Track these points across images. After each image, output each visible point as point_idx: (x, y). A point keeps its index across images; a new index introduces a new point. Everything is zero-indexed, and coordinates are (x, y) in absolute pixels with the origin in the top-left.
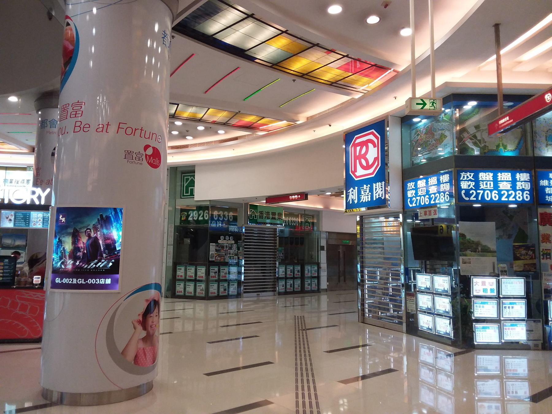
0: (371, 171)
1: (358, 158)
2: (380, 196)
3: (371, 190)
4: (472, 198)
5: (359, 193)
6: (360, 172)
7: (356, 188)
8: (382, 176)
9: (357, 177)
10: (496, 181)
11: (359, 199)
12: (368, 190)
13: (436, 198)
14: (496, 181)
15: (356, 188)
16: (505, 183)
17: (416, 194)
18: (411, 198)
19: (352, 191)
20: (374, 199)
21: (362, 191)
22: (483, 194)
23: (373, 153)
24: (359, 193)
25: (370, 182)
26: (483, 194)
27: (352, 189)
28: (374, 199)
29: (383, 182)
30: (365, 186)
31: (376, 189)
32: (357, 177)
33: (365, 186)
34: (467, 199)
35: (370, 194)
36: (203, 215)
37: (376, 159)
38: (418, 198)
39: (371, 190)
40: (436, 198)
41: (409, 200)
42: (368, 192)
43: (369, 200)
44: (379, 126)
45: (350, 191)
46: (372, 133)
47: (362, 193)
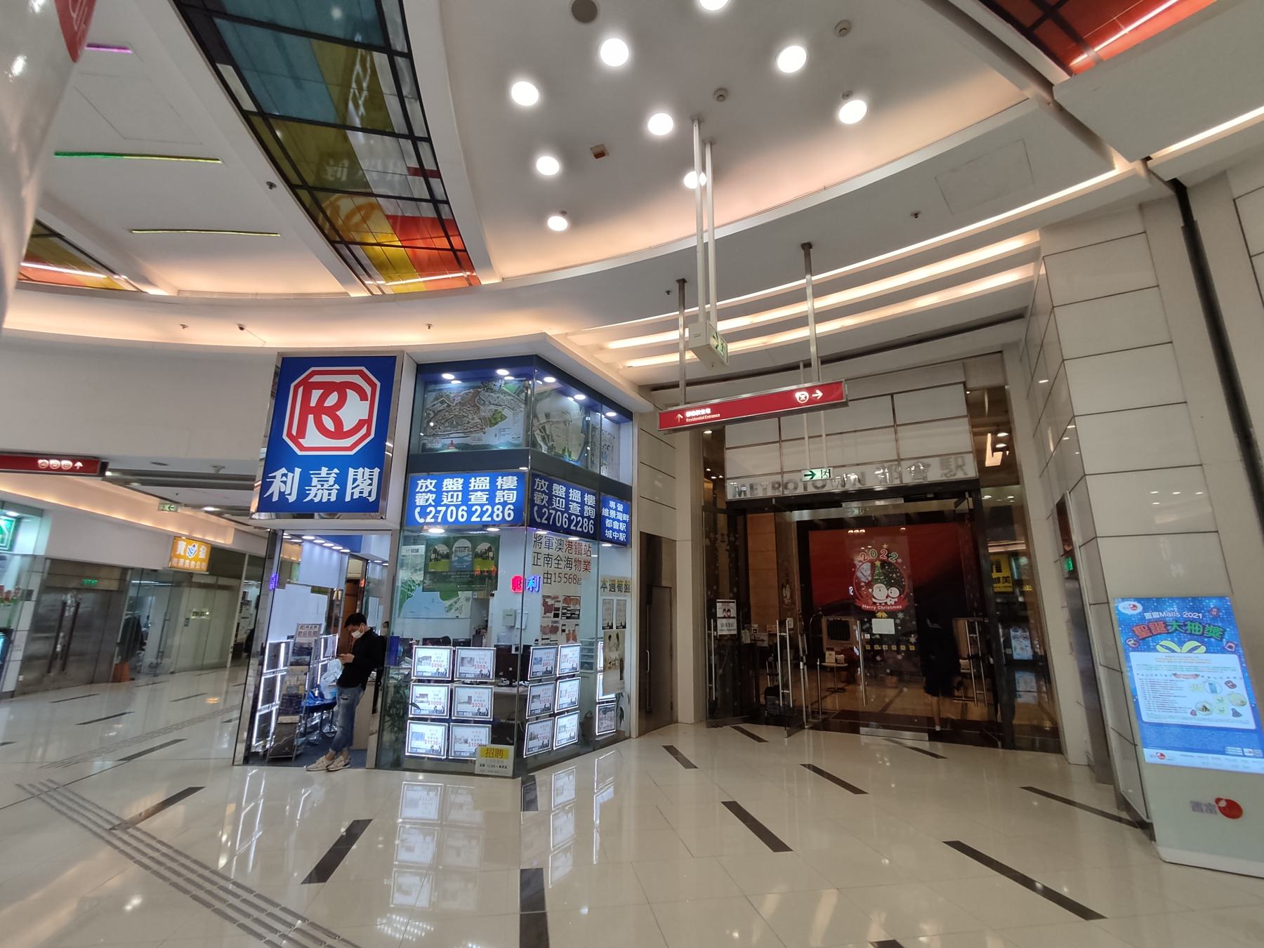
4: (429, 519)
8: (374, 456)
9: (302, 448)
10: (466, 491)
11: (302, 493)
13: (578, 523)
14: (466, 491)
16: (479, 493)
17: (438, 502)
18: (424, 508)
22: (446, 512)
23: (355, 410)
25: (342, 464)
26: (446, 512)
29: (377, 470)
32: (302, 448)
33: (324, 470)
34: (421, 521)
36: (493, 512)
37: (361, 423)
38: (443, 509)
40: (578, 523)
41: (418, 510)
43: (333, 498)
44: (381, 366)
46: (361, 373)
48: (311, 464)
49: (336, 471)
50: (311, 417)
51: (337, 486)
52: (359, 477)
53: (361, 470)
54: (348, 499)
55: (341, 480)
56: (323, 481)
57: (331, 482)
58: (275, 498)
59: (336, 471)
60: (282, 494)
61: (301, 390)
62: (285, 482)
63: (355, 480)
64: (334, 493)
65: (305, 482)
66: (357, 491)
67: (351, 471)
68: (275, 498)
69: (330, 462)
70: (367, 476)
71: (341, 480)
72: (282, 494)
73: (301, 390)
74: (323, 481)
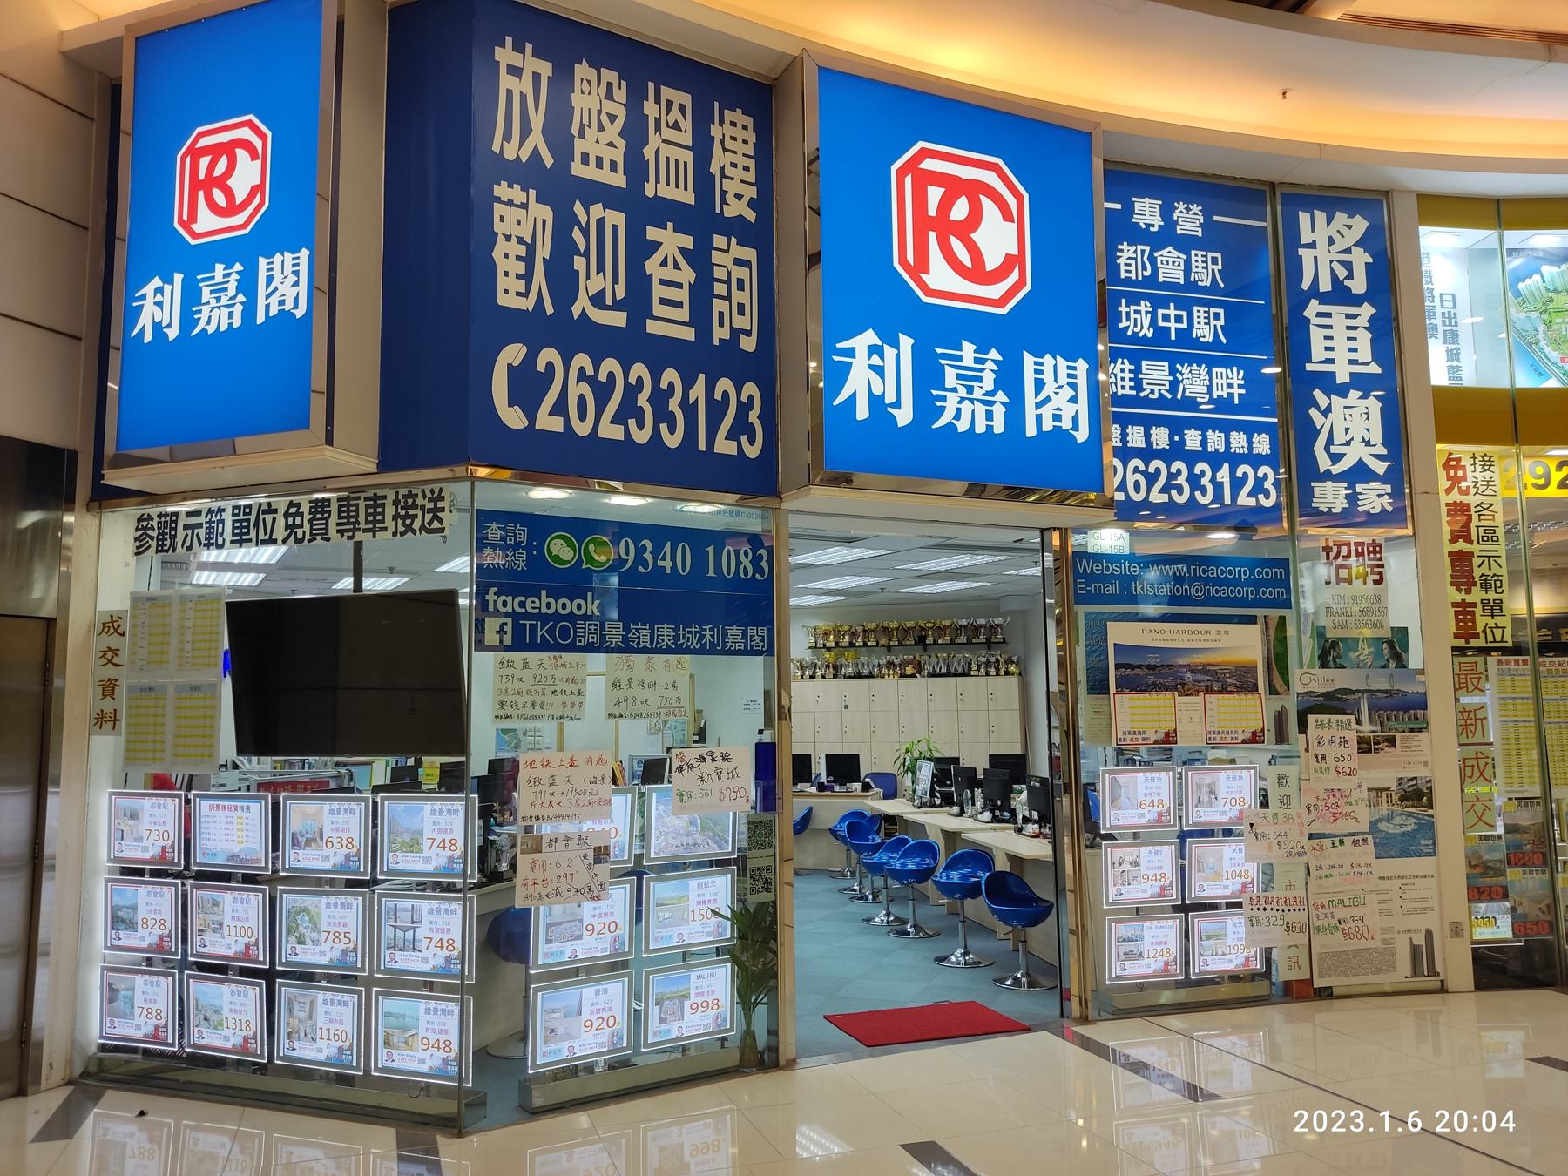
0: (240, 219)
1: (212, 182)
2: (289, 306)
3: (248, 285)
5: (191, 297)
6: (207, 221)
7: (178, 277)
12: (232, 287)
15: (178, 277)
19: (159, 290)
20: (261, 319)
21: (206, 292)
24: (191, 297)
27: (157, 282)
28: (261, 319)
30: (219, 268)
31: (270, 279)
33: (968, 351)
35: (241, 298)
39: (248, 285)
42: (232, 291)
45: (149, 290)
47: (206, 295)
48: (936, 330)
49: (994, 354)
50: (932, 236)
51: (1001, 396)
52: (1048, 377)
53: (1048, 360)
54: (1031, 431)
55: (1009, 378)
56: (970, 378)
57: (989, 384)
58: (862, 412)
59: (994, 354)
60: (876, 401)
61: (908, 180)
62: (879, 370)
63: (1040, 384)
64: (999, 411)
65: (928, 377)
66: (1047, 412)
67: (1028, 360)
68: (862, 412)
69: (983, 330)
70: (1063, 380)
71: (1009, 378)
72: (876, 401)
73: (908, 180)
74: (970, 378)
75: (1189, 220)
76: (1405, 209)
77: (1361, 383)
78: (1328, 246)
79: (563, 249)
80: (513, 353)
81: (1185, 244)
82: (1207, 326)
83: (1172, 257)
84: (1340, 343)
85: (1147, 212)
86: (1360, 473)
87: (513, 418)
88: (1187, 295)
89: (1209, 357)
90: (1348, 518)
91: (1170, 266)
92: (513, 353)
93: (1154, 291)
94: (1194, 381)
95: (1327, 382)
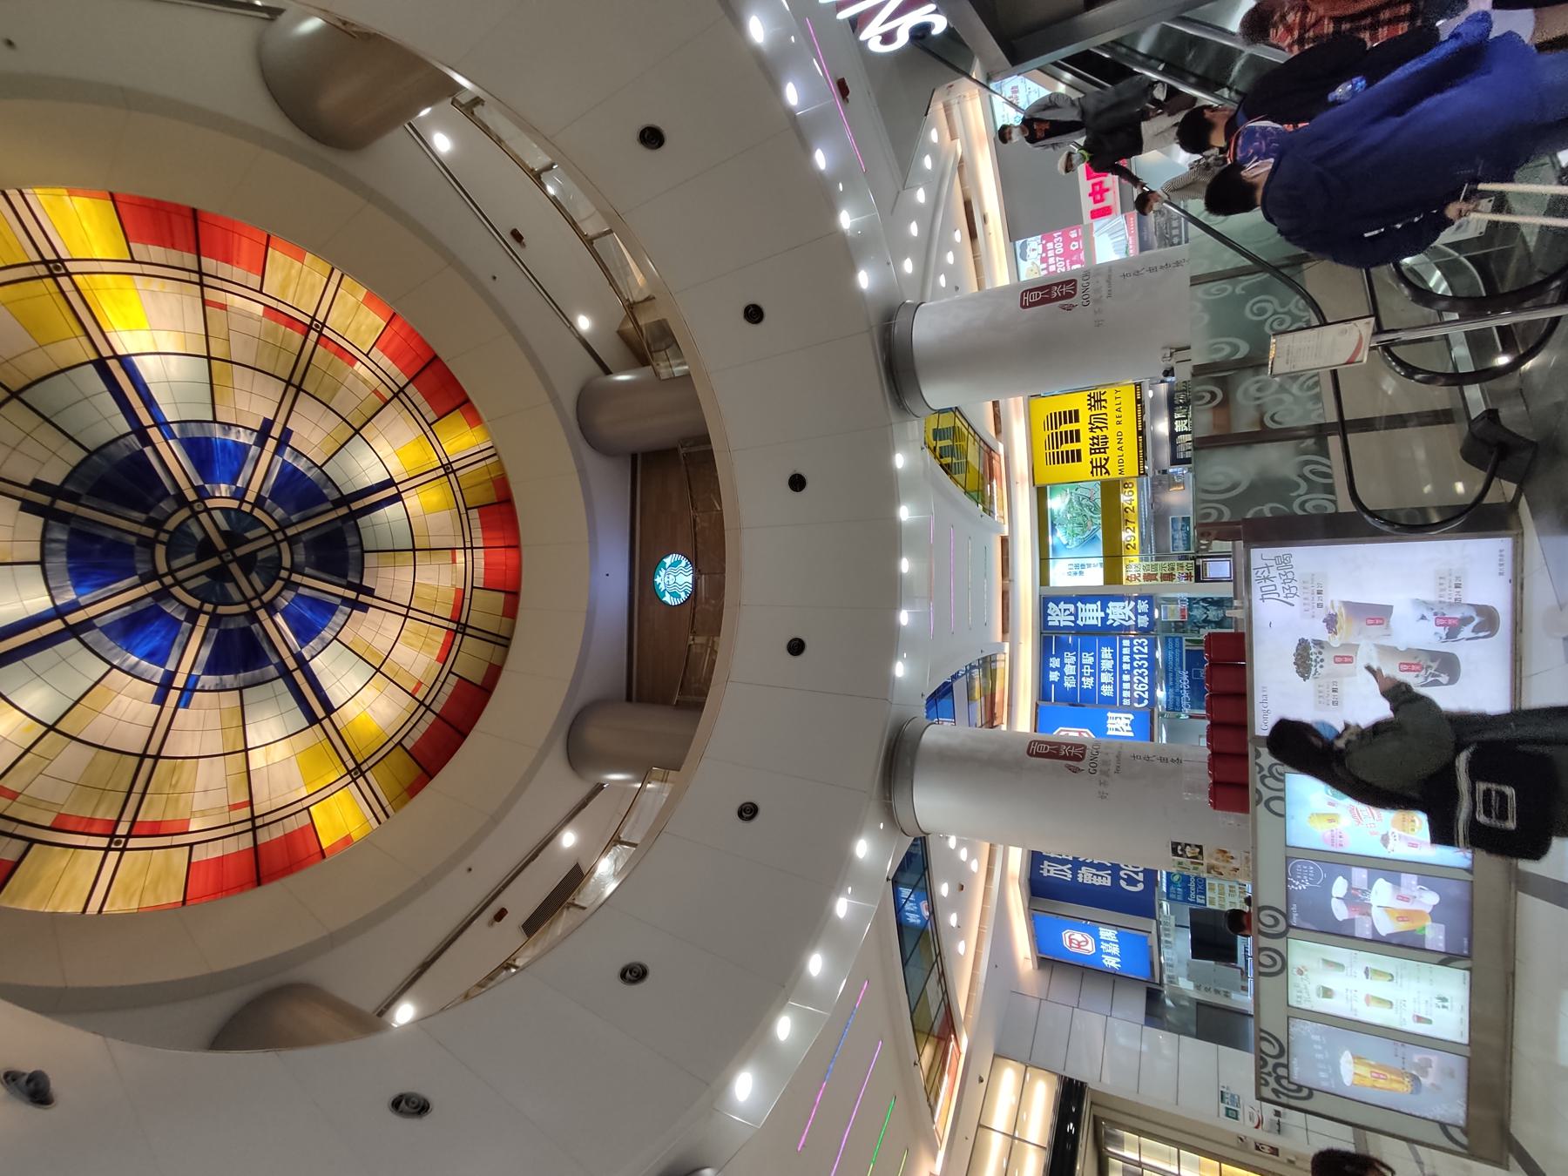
75: (1055, 662)
76: (1047, 592)
77: (1104, 608)
78: (1059, 616)
79: (1091, 865)
80: (1123, 884)
81: (1063, 664)
82: (1088, 659)
83: (1067, 669)
84: (1091, 615)
85: (1054, 676)
86: (1135, 611)
87: (1141, 887)
88: (1079, 665)
89: (1098, 659)
90: (1150, 614)
91: (1070, 669)
92: (1123, 884)
93: (1078, 675)
94: (1107, 664)
95: (1104, 619)
